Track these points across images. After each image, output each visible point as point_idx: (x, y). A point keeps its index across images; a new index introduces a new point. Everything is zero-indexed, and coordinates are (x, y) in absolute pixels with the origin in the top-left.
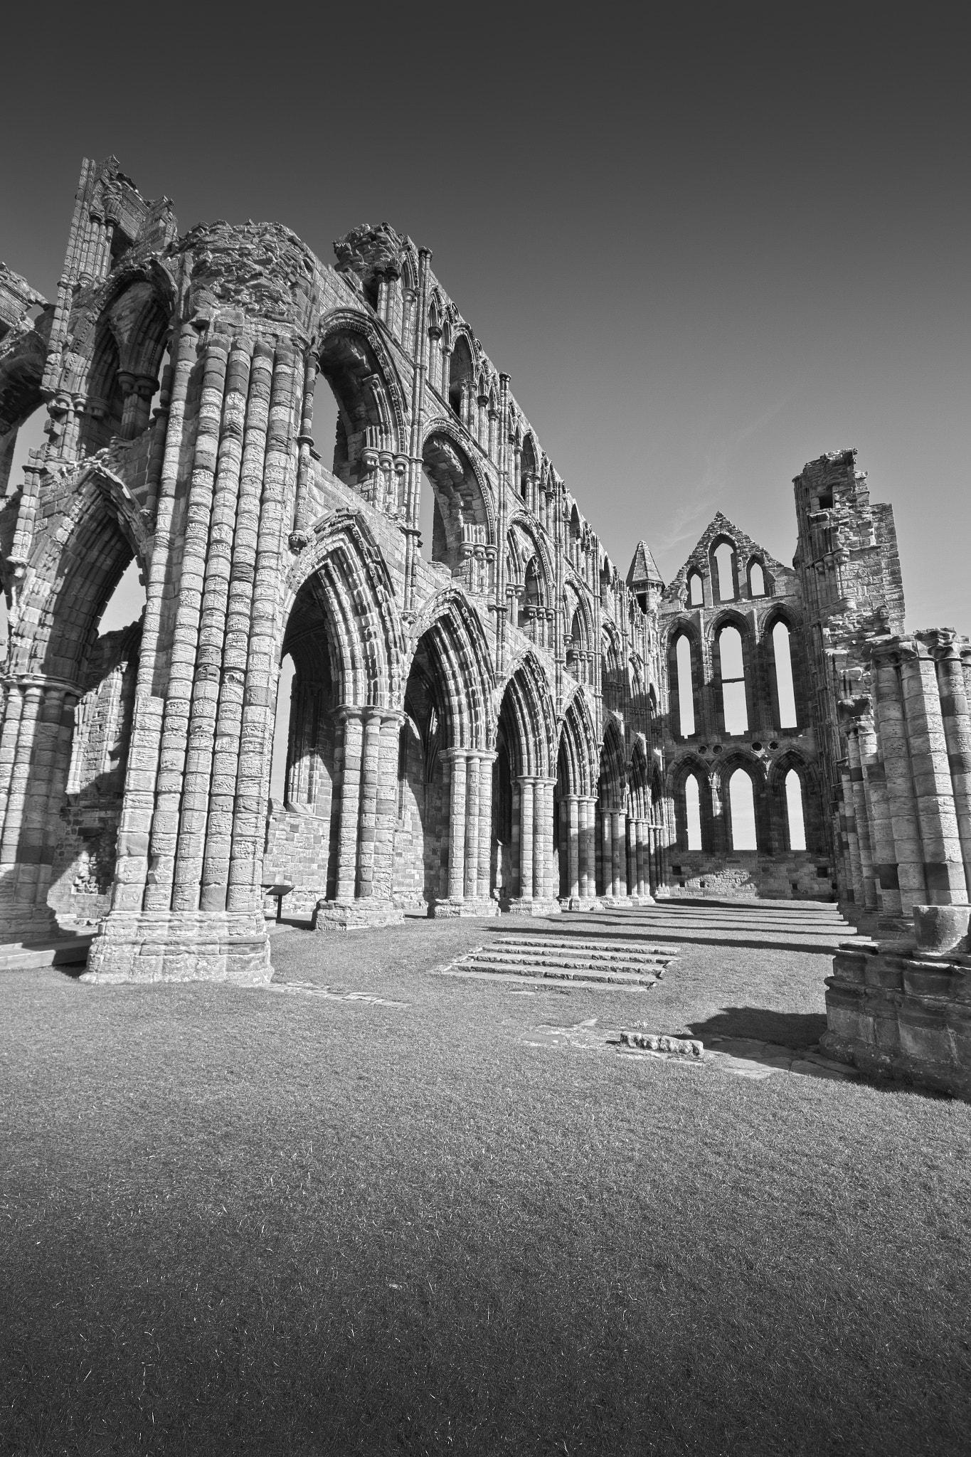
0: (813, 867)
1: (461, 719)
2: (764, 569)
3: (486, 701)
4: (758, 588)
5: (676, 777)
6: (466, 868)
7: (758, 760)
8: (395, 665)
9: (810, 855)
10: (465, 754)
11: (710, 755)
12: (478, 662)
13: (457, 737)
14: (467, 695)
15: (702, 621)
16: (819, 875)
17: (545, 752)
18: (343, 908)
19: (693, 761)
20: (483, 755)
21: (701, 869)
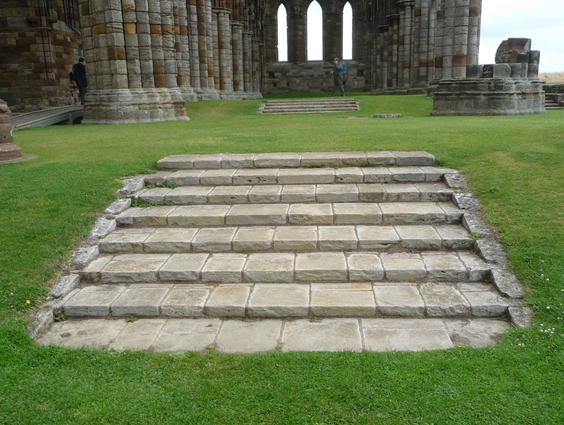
0: (355, 71)
5: (271, 7)
9: (354, 63)
16: (358, 76)
21: (288, 74)
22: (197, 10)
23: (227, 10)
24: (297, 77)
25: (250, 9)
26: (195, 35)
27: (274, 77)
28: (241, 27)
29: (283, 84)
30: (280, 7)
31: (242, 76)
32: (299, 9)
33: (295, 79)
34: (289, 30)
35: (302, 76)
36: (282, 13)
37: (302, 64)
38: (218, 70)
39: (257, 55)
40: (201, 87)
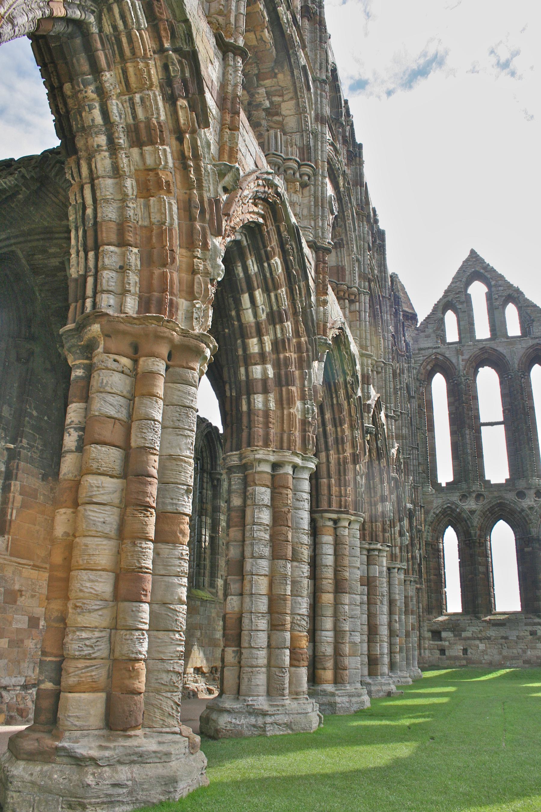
1: (266, 402)
2: (519, 309)
3: (302, 378)
4: (514, 329)
5: (434, 530)
6: (272, 648)
7: (523, 510)
8: (199, 253)
10: (272, 458)
11: (471, 504)
12: (295, 313)
13: (259, 430)
14: (277, 365)
15: (461, 358)
17: (350, 476)
18: (79, 762)
19: (453, 510)
20: (298, 461)
22: (272, 499)
23: (355, 515)
24: (480, 639)
25: (401, 527)
26: (261, 557)
27: (441, 639)
28: (385, 554)
29: (457, 650)
30: (447, 530)
31: (386, 645)
32: (478, 532)
33: (477, 642)
34: (461, 565)
35: (489, 638)
36: (450, 539)
37: (488, 618)
38: (331, 640)
39: (413, 604)
40: (269, 693)
